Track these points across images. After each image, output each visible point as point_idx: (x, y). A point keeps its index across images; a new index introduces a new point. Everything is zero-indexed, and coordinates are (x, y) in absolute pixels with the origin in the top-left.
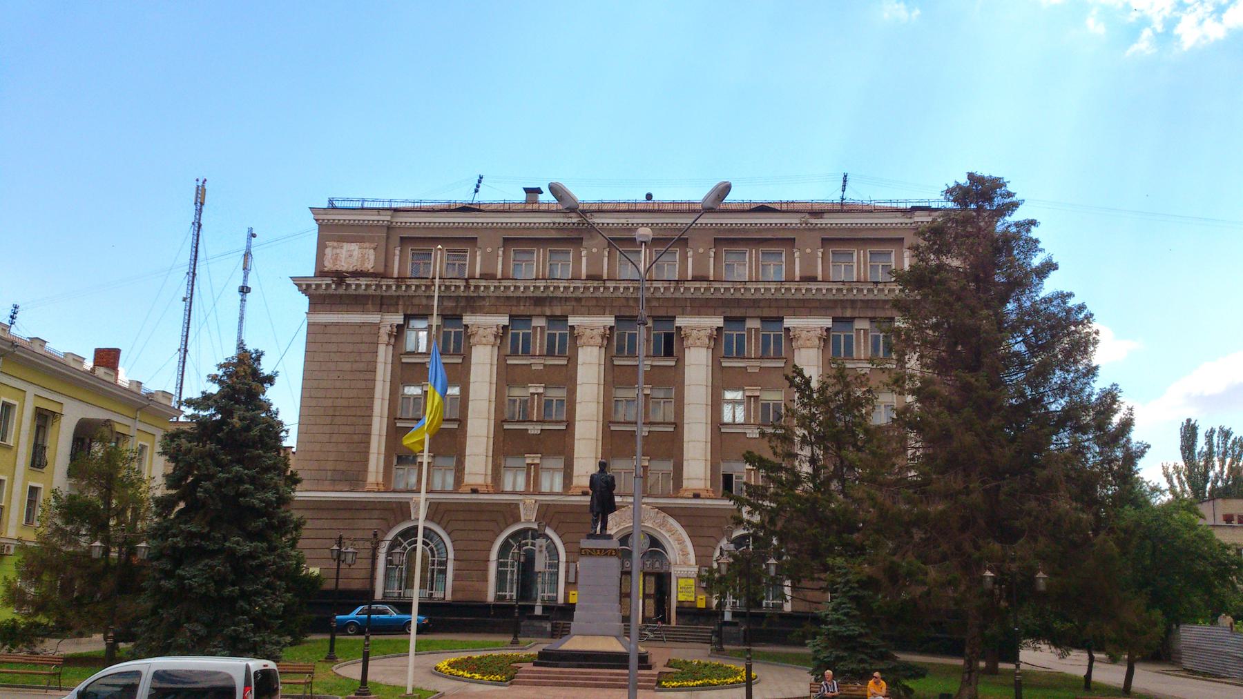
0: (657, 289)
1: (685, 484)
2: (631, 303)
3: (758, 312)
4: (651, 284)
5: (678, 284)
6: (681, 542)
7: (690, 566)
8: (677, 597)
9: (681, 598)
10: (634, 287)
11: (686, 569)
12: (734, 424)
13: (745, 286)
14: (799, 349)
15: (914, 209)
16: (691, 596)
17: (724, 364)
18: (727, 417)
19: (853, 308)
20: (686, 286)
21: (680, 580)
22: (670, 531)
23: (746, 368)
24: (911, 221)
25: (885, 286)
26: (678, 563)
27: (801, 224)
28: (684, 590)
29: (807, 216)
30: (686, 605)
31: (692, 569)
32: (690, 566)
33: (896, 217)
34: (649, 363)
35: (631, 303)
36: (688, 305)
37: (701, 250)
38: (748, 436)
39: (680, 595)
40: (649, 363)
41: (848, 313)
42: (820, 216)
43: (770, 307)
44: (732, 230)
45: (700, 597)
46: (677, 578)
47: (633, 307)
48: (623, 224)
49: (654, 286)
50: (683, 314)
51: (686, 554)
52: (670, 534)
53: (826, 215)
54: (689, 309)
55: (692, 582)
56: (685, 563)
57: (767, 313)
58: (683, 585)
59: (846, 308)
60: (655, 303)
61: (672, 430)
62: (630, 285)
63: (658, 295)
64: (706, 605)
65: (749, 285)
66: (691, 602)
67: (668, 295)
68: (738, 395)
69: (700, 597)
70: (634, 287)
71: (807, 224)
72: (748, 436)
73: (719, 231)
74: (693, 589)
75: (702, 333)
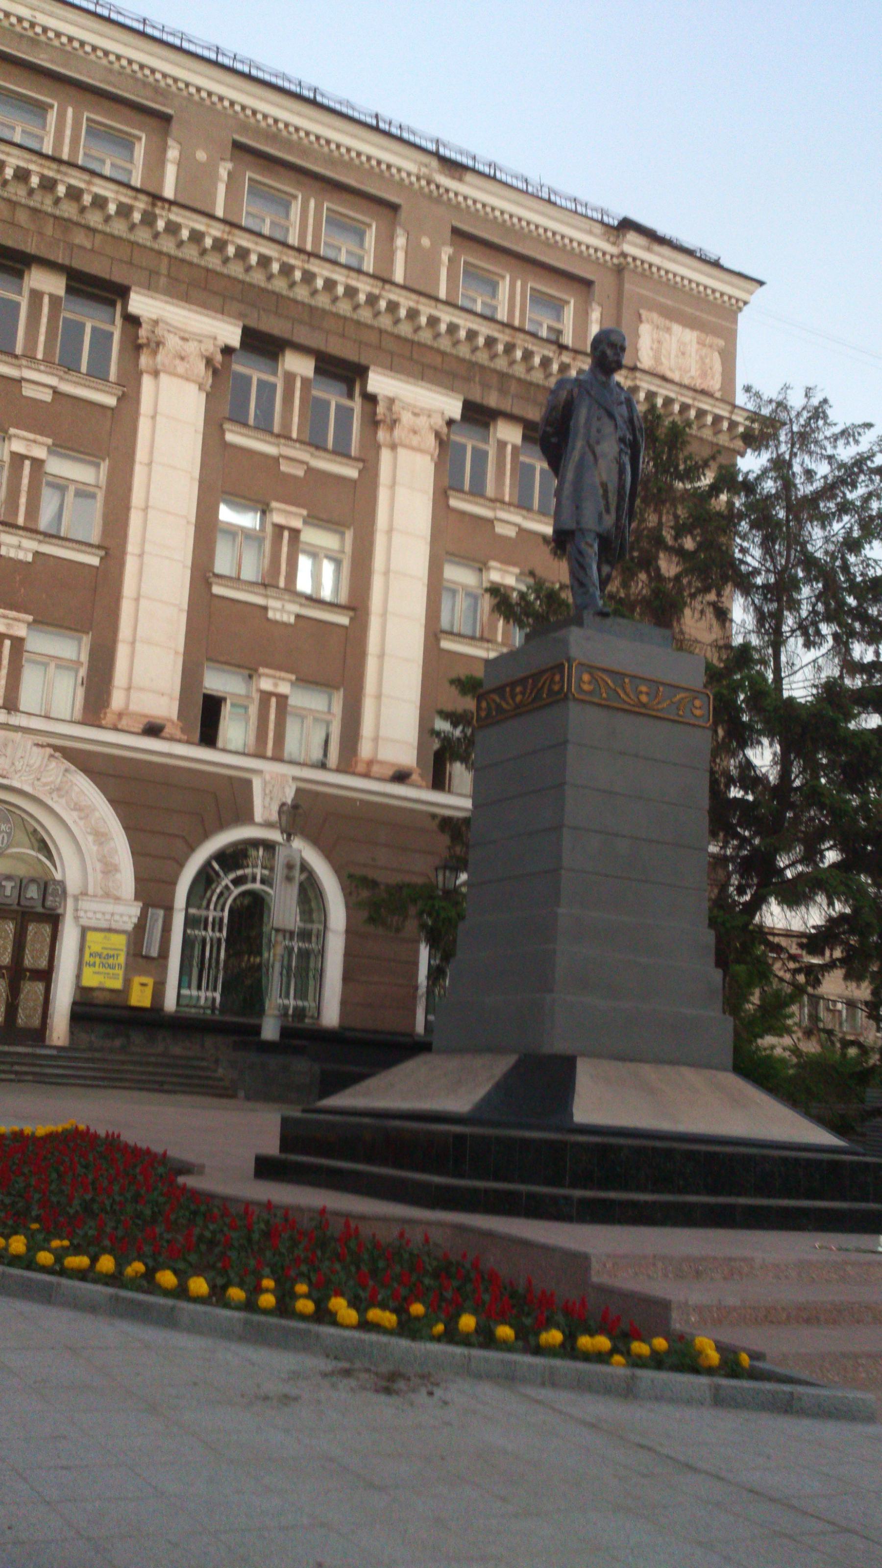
0: (100, 202)
1: (117, 700)
2: (22, 217)
3: (316, 341)
4: (89, 183)
5: (154, 205)
6: (101, 837)
7: (117, 899)
8: (79, 976)
9: (91, 980)
10: (43, 177)
11: (110, 907)
12: (236, 581)
13: (306, 266)
14: (393, 447)
15: (627, 225)
16: (115, 977)
17: (230, 437)
18: (223, 564)
19: (503, 391)
20: (173, 217)
21: (91, 936)
22: (77, 808)
23: (276, 460)
24: (614, 250)
25: (574, 359)
26: (91, 891)
27: (418, 178)
28: (98, 960)
29: (434, 163)
30: (100, 998)
31: (120, 909)
32: (117, 899)
33: (590, 232)
34: (53, 381)
35: (22, 217)
36: (164, 271)
37: (201, 156)
38: (271, 614)
39: (87, 971)
40: (53, 381)
41: (492, 400)
42: (457, 175)
43: (343, 336)
44: (273, 137)
45: (137, 980)
46: (84, 931)
47: (27, 230)
48: (20, 20)
49: (96, 189)
50: (150, 286)
51: (110, 869)
52: (75, 814)
53: (469, 177)
54: (163, 281)
55: (120, 942)
56: (108, 895)
57: (338, 348)
58: (96, 948)
59: (489, 387)
60: (80, 238)
61: (95, 561)
62: (32, 167)
63: (94, 219)
64: (152, 1004)
65: (315, 266)
66: (112, 991)
67: (119, 228)
68: (248, 520)
69: (137, 980)
70: (43, 177)
71: (429, 183)
72: (271, 614)
73: (244, 127)
74: (122, 959)
75: (192, 348)
